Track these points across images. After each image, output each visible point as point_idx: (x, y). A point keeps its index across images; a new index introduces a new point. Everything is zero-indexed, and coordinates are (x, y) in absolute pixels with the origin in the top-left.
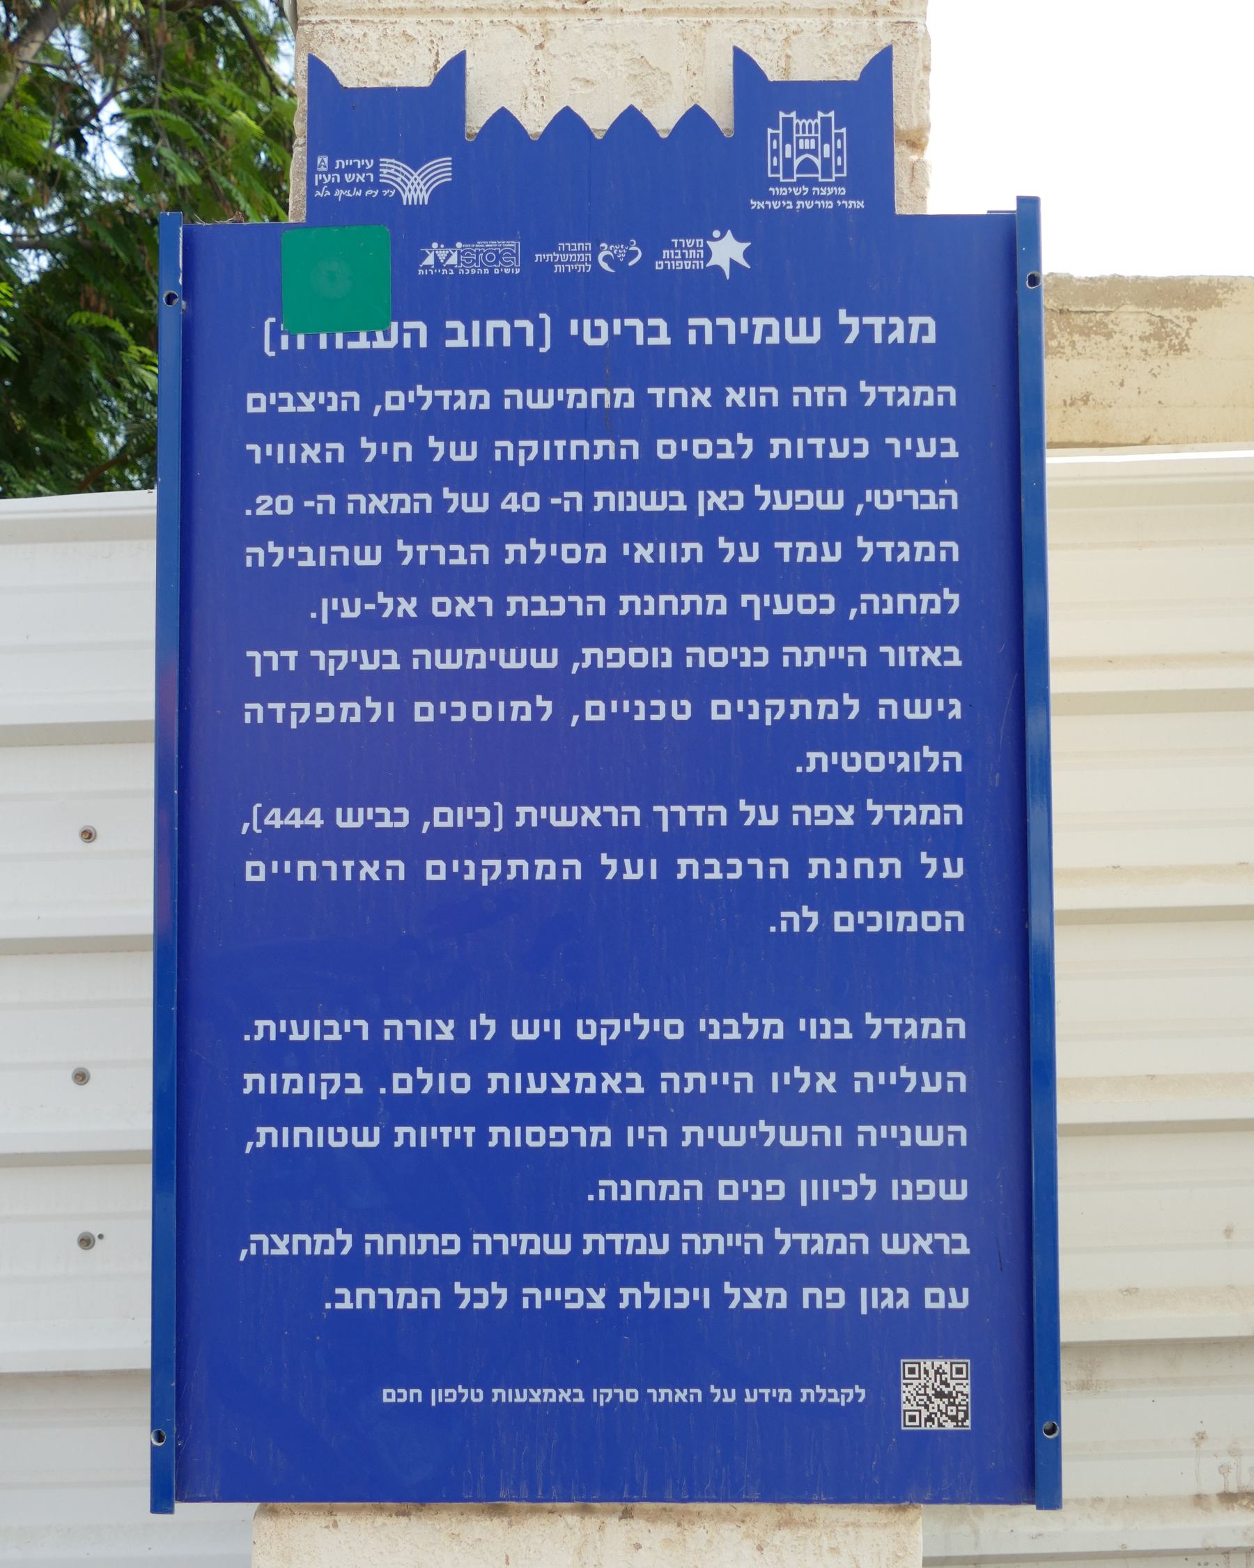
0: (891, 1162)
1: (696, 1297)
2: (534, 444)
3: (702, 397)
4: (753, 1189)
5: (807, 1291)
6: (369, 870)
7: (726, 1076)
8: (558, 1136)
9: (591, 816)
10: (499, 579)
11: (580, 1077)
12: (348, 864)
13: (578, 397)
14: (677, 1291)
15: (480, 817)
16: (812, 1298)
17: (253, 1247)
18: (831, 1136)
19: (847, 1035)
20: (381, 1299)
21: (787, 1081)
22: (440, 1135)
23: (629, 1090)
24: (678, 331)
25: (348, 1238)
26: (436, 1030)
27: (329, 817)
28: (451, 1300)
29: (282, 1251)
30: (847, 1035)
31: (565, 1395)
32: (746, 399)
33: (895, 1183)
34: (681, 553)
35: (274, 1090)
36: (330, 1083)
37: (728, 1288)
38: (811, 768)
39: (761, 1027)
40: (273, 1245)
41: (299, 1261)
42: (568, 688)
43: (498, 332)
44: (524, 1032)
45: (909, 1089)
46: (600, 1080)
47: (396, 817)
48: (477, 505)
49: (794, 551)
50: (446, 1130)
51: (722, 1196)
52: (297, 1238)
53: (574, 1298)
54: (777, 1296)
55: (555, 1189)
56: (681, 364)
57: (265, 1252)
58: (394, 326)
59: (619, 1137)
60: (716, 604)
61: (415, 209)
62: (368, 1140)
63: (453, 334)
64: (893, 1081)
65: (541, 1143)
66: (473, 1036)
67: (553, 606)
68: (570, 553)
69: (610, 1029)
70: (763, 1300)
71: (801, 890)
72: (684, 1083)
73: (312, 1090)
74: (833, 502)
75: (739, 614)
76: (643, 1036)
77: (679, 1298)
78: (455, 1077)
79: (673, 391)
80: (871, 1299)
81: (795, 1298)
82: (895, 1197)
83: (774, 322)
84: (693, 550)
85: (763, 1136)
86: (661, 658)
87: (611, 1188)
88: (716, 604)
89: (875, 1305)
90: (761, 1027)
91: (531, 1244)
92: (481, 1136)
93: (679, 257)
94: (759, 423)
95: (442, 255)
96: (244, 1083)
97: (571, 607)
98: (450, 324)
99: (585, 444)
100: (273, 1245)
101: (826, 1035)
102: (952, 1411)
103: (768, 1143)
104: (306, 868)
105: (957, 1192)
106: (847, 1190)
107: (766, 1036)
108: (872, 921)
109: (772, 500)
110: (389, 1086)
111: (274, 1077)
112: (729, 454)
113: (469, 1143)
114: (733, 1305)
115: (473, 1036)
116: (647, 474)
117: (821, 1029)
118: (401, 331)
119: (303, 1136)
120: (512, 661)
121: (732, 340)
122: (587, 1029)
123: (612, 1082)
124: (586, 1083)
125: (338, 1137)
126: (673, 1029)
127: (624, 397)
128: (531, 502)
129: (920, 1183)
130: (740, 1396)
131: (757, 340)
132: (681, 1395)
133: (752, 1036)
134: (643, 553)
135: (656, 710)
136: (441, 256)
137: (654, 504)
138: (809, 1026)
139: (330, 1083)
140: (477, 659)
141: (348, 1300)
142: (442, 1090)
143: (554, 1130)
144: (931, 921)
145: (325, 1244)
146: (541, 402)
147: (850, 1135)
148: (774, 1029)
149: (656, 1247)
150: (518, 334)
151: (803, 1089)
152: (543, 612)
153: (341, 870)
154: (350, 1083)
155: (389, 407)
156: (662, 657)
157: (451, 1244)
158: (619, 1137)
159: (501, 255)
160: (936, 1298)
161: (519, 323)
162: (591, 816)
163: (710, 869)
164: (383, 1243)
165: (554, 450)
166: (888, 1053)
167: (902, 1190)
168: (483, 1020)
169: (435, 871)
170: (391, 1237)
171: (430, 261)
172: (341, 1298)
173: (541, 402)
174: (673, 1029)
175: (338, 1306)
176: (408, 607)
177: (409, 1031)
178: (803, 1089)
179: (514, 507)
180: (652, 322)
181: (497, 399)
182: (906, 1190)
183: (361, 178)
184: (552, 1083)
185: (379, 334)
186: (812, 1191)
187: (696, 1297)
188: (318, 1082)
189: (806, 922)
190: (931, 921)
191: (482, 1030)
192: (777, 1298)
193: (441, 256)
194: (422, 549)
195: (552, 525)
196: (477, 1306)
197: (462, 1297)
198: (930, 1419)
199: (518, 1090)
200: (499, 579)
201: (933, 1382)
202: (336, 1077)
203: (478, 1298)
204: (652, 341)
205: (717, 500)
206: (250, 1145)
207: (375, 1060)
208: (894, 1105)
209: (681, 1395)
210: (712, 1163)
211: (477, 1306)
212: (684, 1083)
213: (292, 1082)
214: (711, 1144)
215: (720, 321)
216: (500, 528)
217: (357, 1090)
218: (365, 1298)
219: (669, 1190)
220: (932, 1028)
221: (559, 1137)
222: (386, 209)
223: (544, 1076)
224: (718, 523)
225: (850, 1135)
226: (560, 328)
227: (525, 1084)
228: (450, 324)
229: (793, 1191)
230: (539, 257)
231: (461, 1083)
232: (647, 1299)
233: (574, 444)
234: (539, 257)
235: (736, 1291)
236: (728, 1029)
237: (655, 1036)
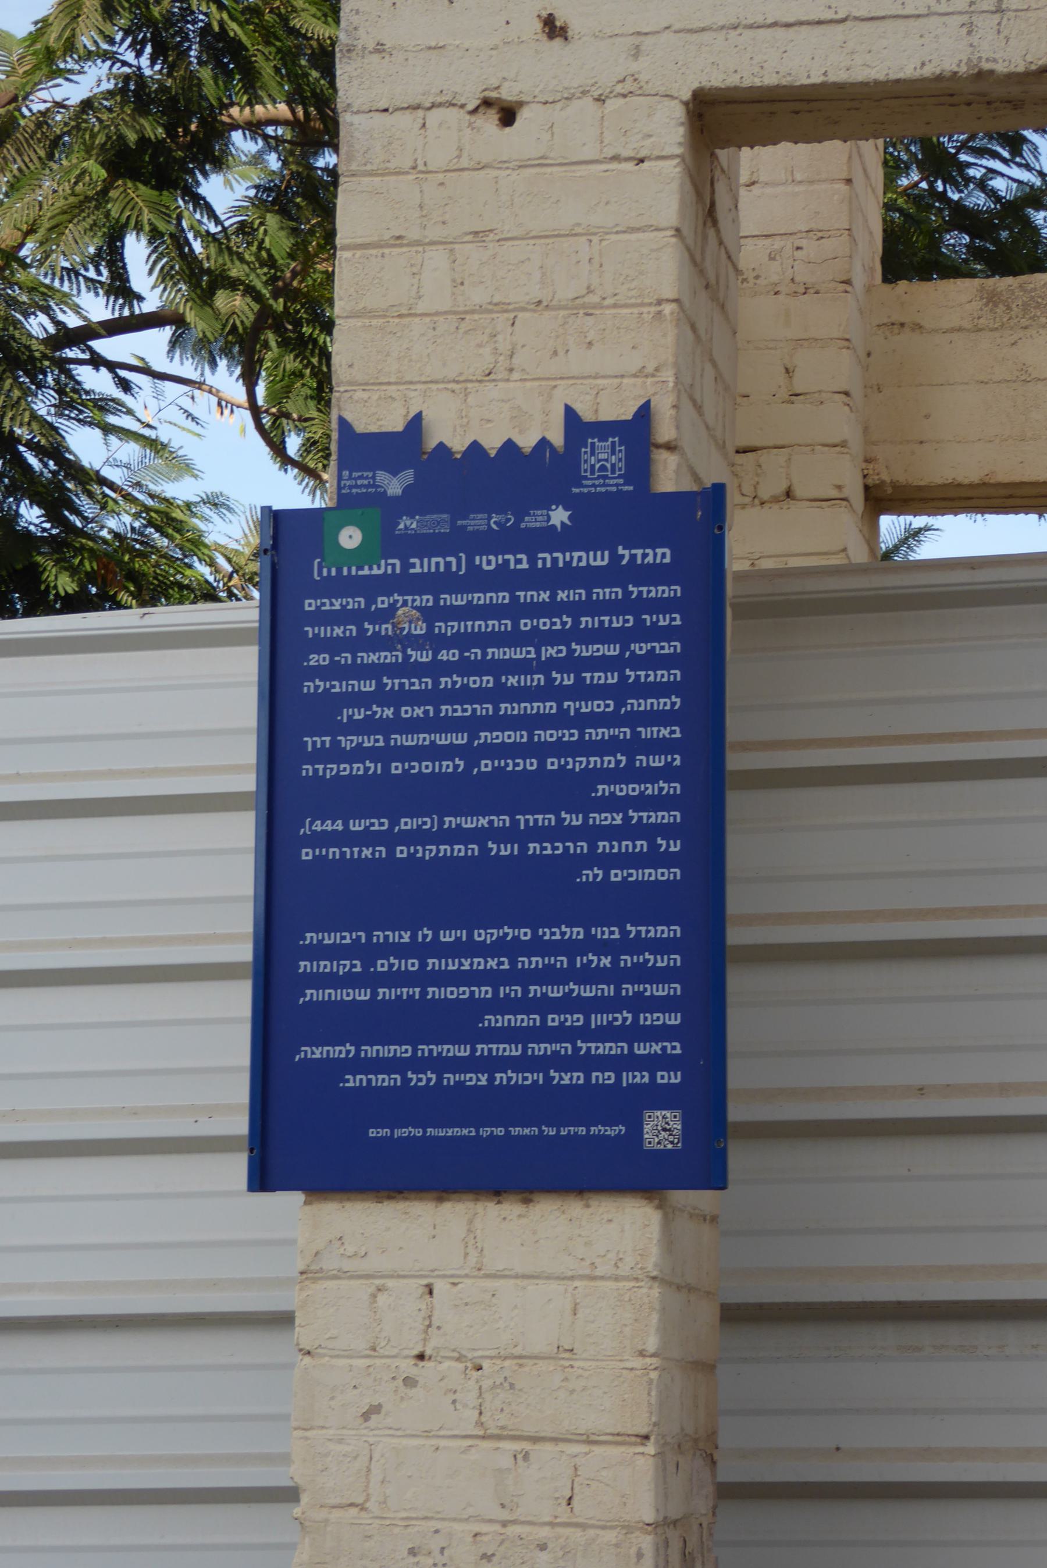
0: (640, 1004)
1: (535, 1078)
2: (456, 624)
3: (545, 596)
4: (566, 1020)
5: (594, 1074)
6: (367, 853)
7: (553, 959)
8: (463, 992)
9: (484, 822)
10: (436, 697)
11: (476, 960)
12: (356, 850)
13: (480, 598)
14: (526, 1075)
15: (425, 823)
16: (597, 1077)
17: (303, 1054)
18: (608, 990)
19: (617, 936)
20: (369, 1081)
21: (585, 961)
22: (402, 992)
23: (502, 967)
24: (533, 561)
25: (353, 1048)
26: (401, 937)
27: (346, 824)
28: (406, 1081)
29: (318, 1056)
30: (617, 936)
31: (465, 1132)
32: (568, 596)
33: (642, 1015)
34: (532, 680)
35: (315, 970)
36: (345, 966)
37: (552, 1073)
38: (599, 794)
39: (572, 932)
40: (313, 1053)
41: (327, 1061)
42: (472, 754)
43: (437, 564)
44: (447, 937)
45: (650, 965)
46: (486, 962)
47: (381, 824)
48: (425, 657)
49: (592, 678)
50: (405, 990)
51: (550, 1024)
52: (326, 1048)
53: (471, 1079)
54: (578, 1077)
55: (461, 1023)
56: (534, 579)
57: (309, 1056)
58: (383, 562)
59: (496, 992)
60: (550, 707)
61: (396, 498)
62: (364, 996)
63: (413, 566)
64: (641, 960)
65: (454, 996)
66: (420, 940)
67: (465, 710)
68: (474, 682)
69: (492, 935)
70: (571, 1079)
71: (593, 859)
72: (530, 963)
73: (335, 970)
74: (612, 651)
75: (562, 712)
76: (509, 938)
77: (525, 1079)
78: (410, 961)
79: (529, 593)
80: (629, 1078)
81: (588, 1078)
82: (642, 1023)
83: (583, 554)
84: (539, 678)
85: (572, 991)
86: (521, 737)
87: (492, 1020)
88: (550, 707)
89: (630, 1081)
90: (572, 932)
91: (448, 1050)
92: (424, 993)
93: (533, 521)
94: (575, 609)
95: (408, 523)
96: (299, 967)
97: (474, 710)
98: (412, 560)
99: (482, 623)
100: (313, 1053)
101: (606, 937)
102: (671, 1138)
103: (574, 995)
104: (334, 852)
105: (674, 1020)
106: (616, 1019)
107: (574, 937)
108: (631, 875)
109: (581, 650)
110: (375, 967)
111: (315, 963)
112: (558, 627)
113: (417, 997)
114: (555, 1082)
115: (420, 940)
116: (515, 639)
117: (603, 933)
118: (387, 565)
119: (330, 994)
120: (442, 740)
121: (561, 565)
122: (480, 935)
123: (492, 963)
124: (479, 964)
125: (348, 995)
126: (525, 934)
127: (503, 597)
128: (454, 655)
129: (655, 1015)
130: (558, 1131)
131: (574, 564)
132: (527, 1131)
133: (566, 937)
134: (513, 681)
135: (518, 765)
136: (408, 524)
137: (519, 654)
138: (597, 932)
139: (345, 966)
140: (424, 739)
141: (352, 1081)
142: (403, 969)
143: (462, 989)
144: (662, 874)
145: (340, 1052)
146: (459, 601)
147: (618, 990)
148: (578, 933)
149: (514, 1051)
150: (448, 565)
151: (593, 966)
152: (459, 714)
153: (352, 853)
154: (355, 966)
155: (380, 606)
156: (522, 737)
157: (406, 1051)
158: (496, 992)
159: (439, 523)
160: (663, 1078)
161: (448, 559)
162: (484, 822)
163: (546, 849)
164: (371, 1051)
165: (466, 627)
166: (640, 945)
167: (646, 1019)
168: (426, 931)
169: (401, 852)
170: (375, 1048)
171: (401, 526)
172: (348, 1081)
173: (459, 601)
174: (525, 934)
175: (347, 1085)
176: (389, 712)
177: (386, 937)
178: (593, 966)
179: (445, 658)
180: (519, 556)
181: (436, 600)
182: (647, 1019)
183: (366, 482)
184: (461, 964)
185: (375, 567)
186: (598, 1020)
187: (535, 1078)
188: (338, 965)
189: (596, 876)
190: (662, 874)
191: (425, 936)
192: (578, 1078)
193: (408, 524)
194: (397, 681)
195: (465, 667)
196: (420, 1084)
197: (411, 1079)
198: (659, 1143)
199: (443, 968)
200: (436, 697)
201: (661, 1123)
202: (347, 962)
203: (420, 1080)
204: (519, 567)
205: (552, 651)
206: (302, 1000)
207: (369, 953)
208: (643, 974)
209: (527, 1131)
210: (544, 1006)
211: (420, 1084)
212: (530, 963)
213: (325, 966)
214: (544, 995)
215: (555, 555)
216: (436, 669)
217: (358, 969)
218: (361, 1080)
219: (522, 1020)
220: (663, 931)
221: (464, 993)
222: (379, 499)
223: (457, 960)
224: (552, 664)
225: (618, 990)
226: (470, 561)
227: (447, 965)
228: (412, 560)
229: (587, 1021)
230: (459, 523)
231: (413, 965)
232: (509, 1079)
233: (477, 623)
234: (459, 523)
235: (557, 1075)
236: (553, 934)
237: (516, 938)
